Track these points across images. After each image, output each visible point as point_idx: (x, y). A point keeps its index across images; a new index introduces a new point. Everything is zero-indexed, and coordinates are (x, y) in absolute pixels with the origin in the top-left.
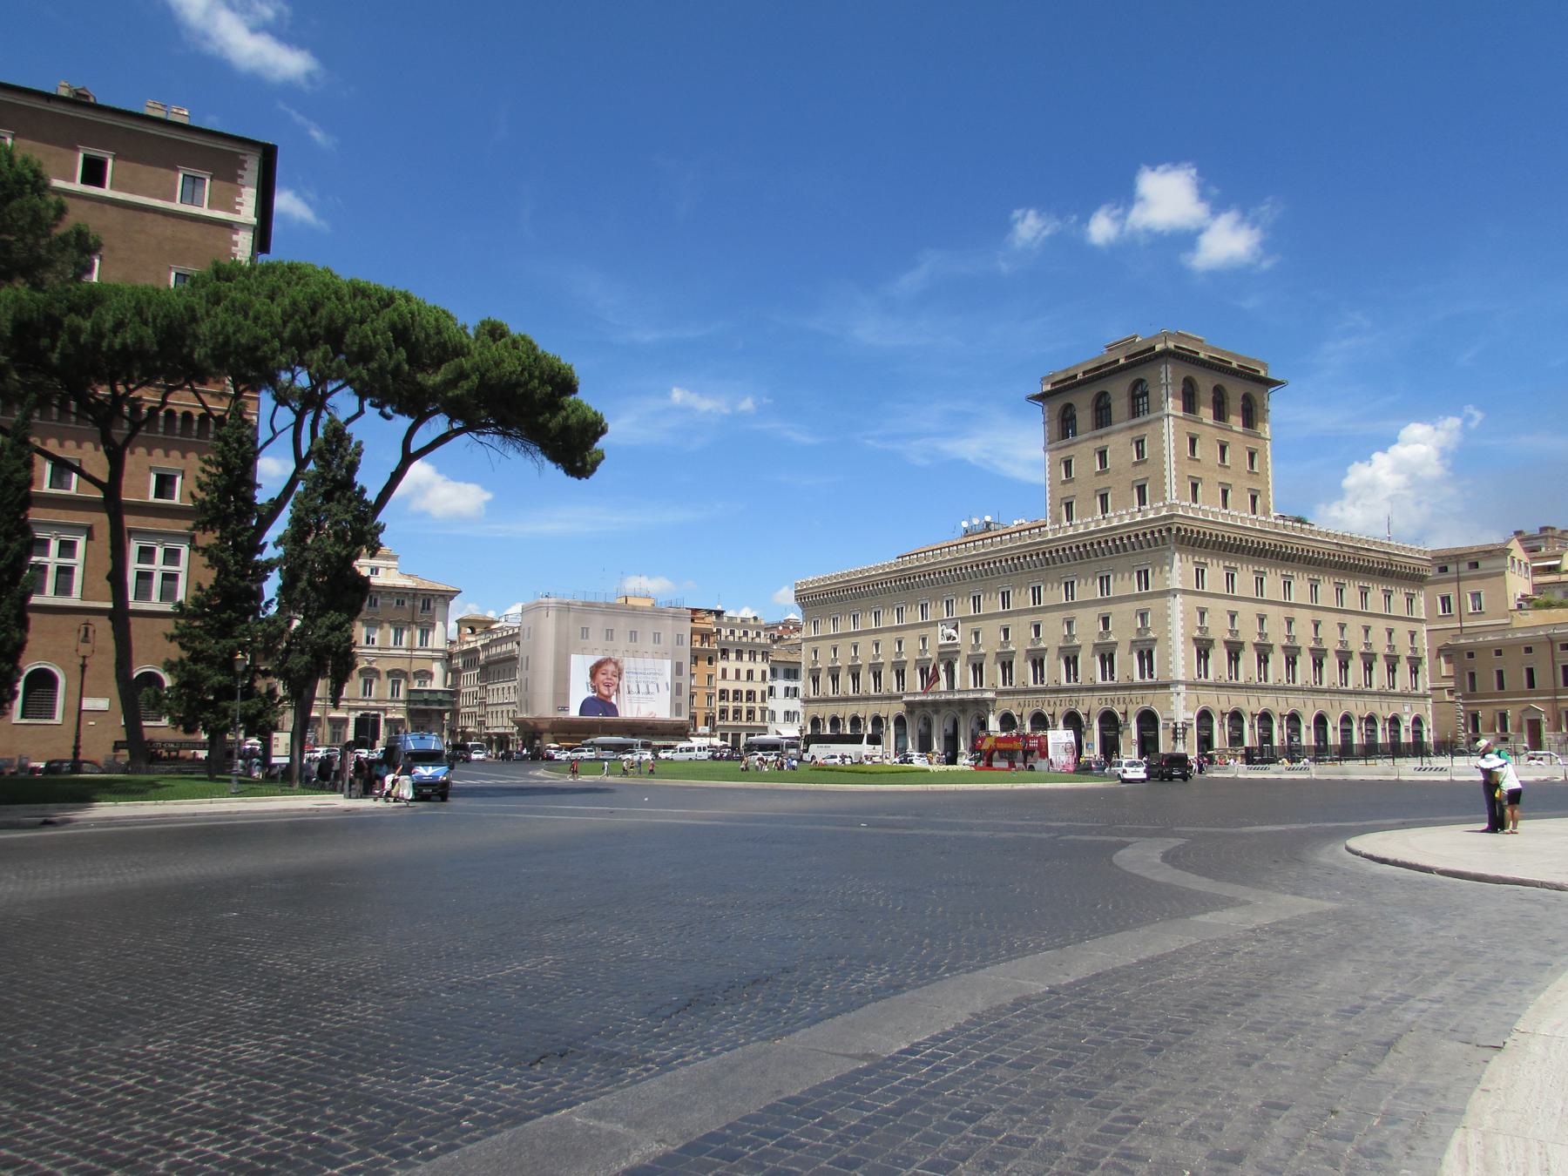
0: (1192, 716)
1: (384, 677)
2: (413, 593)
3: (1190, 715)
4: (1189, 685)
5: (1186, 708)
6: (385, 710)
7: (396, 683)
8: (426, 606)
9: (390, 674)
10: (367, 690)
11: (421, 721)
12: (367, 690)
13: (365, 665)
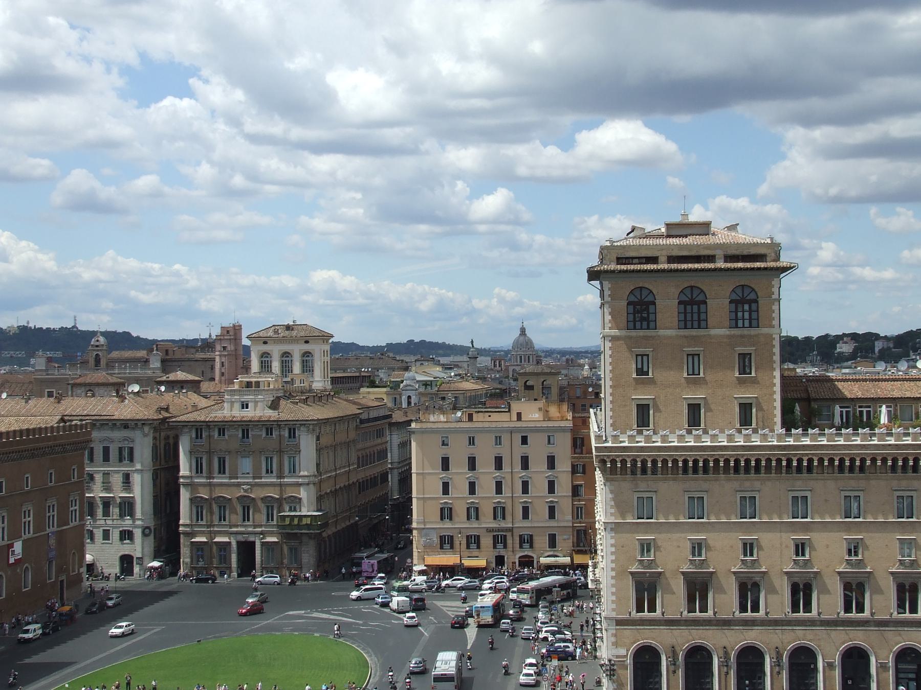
0: (626, 653)
1: (260, 504)
2: (279, 424)
3: (623, 652)
4: (619, 622)
5: (616, 644)
6: (261, 533)
7: (270, 509)
8: (292, 433)
9: (264, 499)
10: (246, 517)
11: (293, 543)
12: (246, 517)
13: (242, 493)
